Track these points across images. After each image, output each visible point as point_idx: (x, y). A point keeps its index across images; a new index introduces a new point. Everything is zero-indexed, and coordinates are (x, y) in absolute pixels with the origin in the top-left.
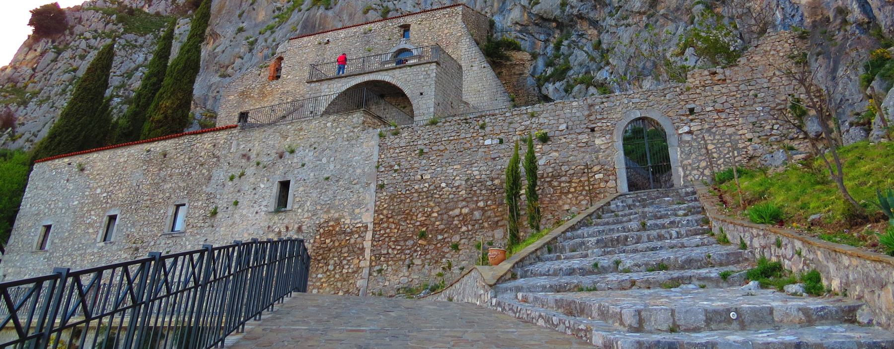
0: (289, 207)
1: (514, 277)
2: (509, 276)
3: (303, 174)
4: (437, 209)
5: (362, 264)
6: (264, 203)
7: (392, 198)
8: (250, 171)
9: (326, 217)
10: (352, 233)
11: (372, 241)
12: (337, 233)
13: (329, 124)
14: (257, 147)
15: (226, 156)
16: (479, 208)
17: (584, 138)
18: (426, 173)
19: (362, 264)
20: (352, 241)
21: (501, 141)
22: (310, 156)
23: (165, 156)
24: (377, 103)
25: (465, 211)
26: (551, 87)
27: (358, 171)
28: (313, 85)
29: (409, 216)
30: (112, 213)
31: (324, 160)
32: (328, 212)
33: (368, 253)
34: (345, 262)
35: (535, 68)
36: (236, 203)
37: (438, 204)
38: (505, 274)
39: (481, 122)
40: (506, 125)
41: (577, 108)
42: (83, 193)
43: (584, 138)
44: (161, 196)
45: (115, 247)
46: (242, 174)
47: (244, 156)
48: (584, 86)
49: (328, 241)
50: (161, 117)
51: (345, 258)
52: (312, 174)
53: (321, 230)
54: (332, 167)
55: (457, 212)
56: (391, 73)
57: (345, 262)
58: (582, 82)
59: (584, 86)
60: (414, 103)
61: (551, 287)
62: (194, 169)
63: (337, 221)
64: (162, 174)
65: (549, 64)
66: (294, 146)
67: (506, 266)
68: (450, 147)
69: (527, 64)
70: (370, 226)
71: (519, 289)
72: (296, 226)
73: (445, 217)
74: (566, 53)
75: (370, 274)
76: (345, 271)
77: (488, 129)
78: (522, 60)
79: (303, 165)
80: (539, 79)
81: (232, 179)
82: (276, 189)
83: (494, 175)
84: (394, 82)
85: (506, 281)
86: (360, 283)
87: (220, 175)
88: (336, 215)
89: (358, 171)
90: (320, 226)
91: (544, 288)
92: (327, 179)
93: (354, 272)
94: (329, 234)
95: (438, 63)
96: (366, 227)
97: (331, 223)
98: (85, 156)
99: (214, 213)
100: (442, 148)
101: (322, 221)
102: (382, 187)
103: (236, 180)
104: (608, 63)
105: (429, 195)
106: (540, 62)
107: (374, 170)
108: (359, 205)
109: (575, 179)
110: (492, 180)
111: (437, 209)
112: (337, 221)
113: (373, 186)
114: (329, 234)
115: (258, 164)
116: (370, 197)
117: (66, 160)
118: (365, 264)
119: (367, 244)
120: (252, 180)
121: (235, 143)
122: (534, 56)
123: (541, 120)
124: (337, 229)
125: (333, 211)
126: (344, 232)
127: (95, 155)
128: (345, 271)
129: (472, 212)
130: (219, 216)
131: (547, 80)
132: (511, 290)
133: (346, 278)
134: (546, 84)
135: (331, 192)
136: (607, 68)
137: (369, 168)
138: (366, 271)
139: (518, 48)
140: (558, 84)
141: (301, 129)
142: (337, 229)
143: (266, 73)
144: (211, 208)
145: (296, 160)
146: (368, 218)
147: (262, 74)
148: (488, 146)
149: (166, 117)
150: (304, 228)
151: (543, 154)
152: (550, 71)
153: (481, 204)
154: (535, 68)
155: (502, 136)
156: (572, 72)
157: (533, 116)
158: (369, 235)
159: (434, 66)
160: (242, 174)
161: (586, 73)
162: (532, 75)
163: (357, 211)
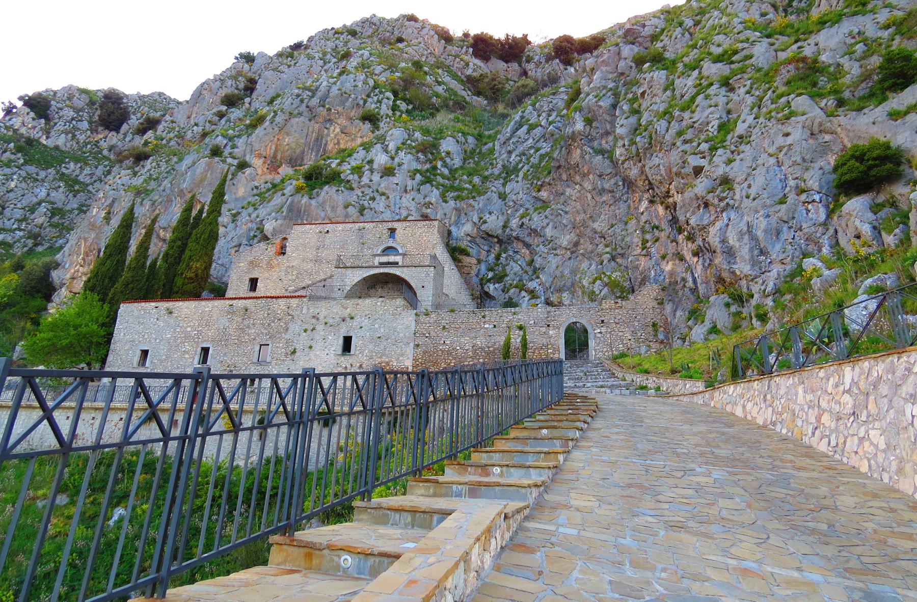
0: (352, 352)
3: (361, 333)
7: (425, 352)
8: (320, 327)
9: (379, 360)
14: (323, 313)
15: (298, 316)
18: (448, 340)
21: (495, 326)
27: (401, 335)
31: (377, 326)
32: (381, 357)
36: (311, 347)
46: (313, 329)
47: (314, 317)
54: (382, 330)
62: (273, 322)
66: (353, 315)
68: (463, 326)
77: (487, 319)
81: (305, 331)
87: (295, 327)
89: (401, 335)
99: (294, 352)
102: (418, 345)
103: (309, 332)
105: (449, 353)
108: (402, 355)
113: (412, 345)
116: (410, 351)
120: (322, 333)
121: (305, 308)
130: (298, 354)
137: (409, 333)
144: (291, 349)
150: (364, 366)
160: (313, 329)
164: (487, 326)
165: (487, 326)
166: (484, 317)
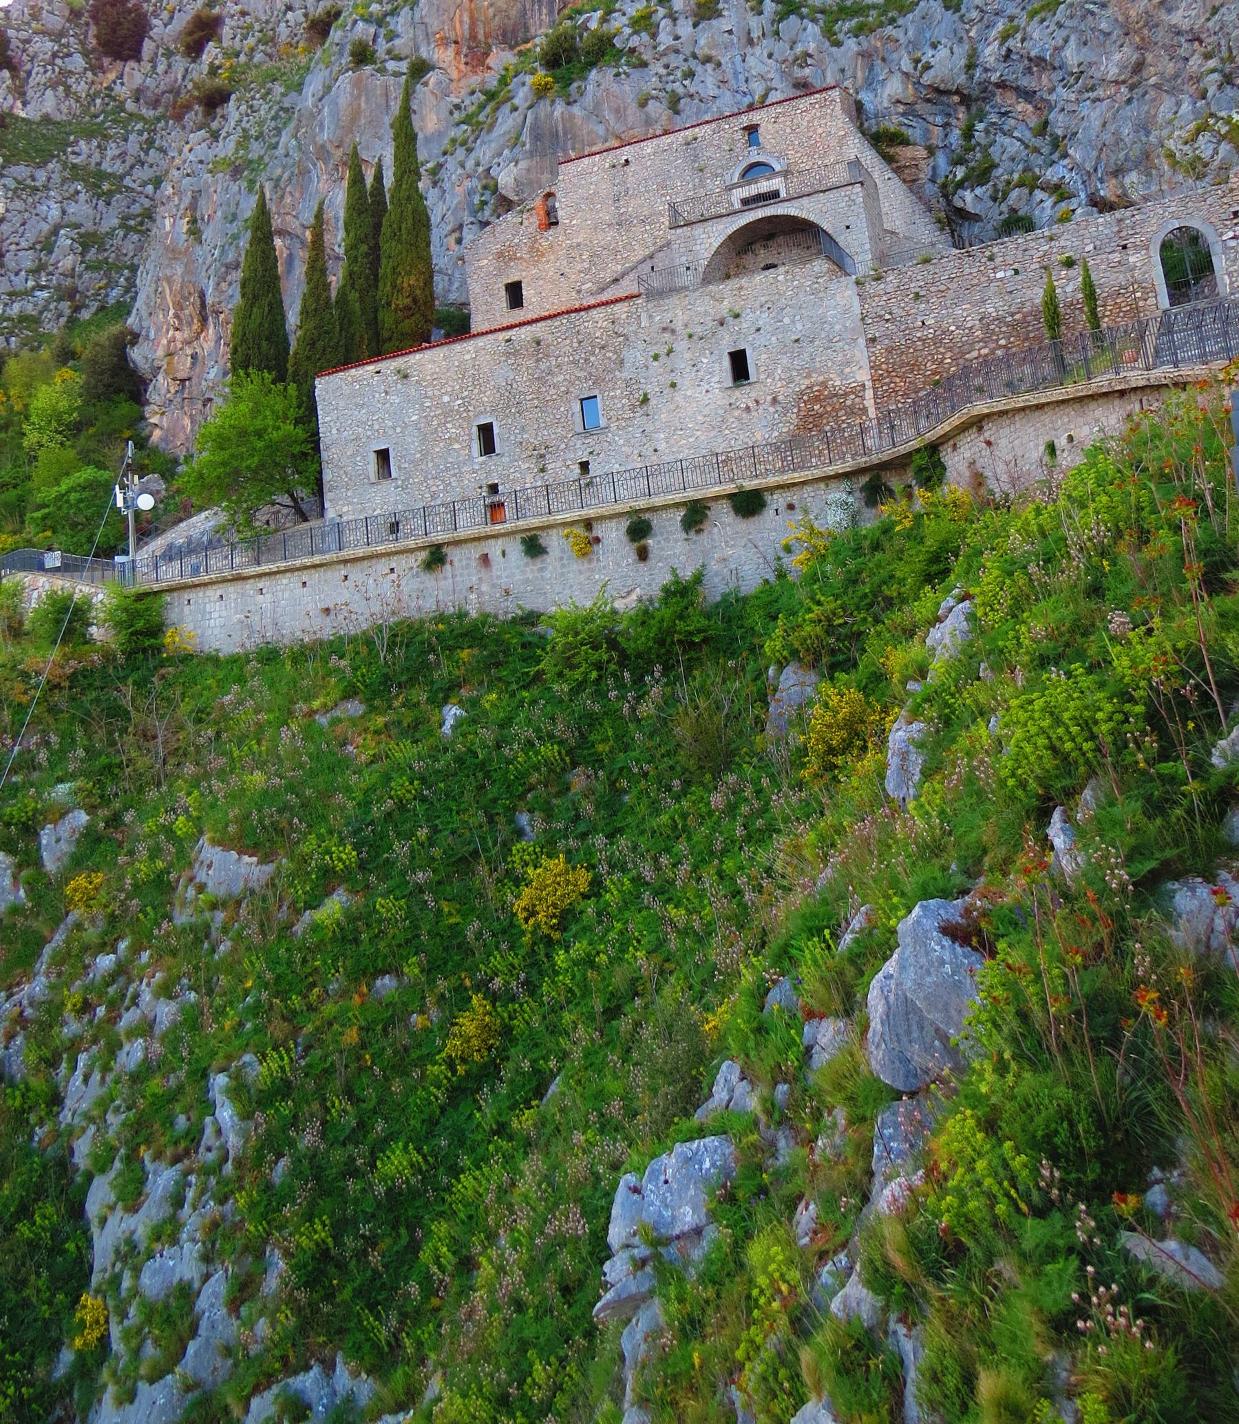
0: (752, 378)
3: (761, 340)
4: (949, 355)
6: (716, 379)
7: (889, 350)
8: (681, 345)
9: (807, 382)
10: (846, 394)
11: (875, 396)
12: (826, 397)
13: (781, 278)
14: (680, 319)
15: (636, 333)
16: (1001, 347)
17: (1116, 257)
18: (931, 317)
20: (849, 403)
21: (1017, 272)
22: (764, 319)
23: (538, 343)
24: (765, 247)
25: (985, 351)
26: (968, 195)
27: (838, 327)
28: (679, 231)
29: (915, 366)
31: (786, 320)
32: (808, 376)
33: (872, 413)
35: (934, 169)
36: (673, 385)
37: (950, 349)
39: (988, 253)
40: (1020, 253)
41: (1106, 224)
43: (1116, 257)
44: (552, 391)
45: (505, 459)
46: (670, 351)
47: (665, 329)
48: (1026, 191)
50: (408, 301)
54: (799, 327)
55: (975, 354)
56: (796, 203)
58: (1020, 185)
59: (1026, 191)
60: (841, 240)
62: (593, 354)
63: (824, 384)
64: (543, 366)
65: (960, 161)
66: (737, 310)
68: (953, 286)
69: (922, 164)
70: (869, 384)
72: (769, 398)
73: (961, 361)
74: (983, 142)
77: (998, 260)
78: (913, 159)
80: (944, 186)
81: (656, 358)
82: (726, 363)
83: (1013, 309)
84: (804, 215)
87: (635, 356)
88: (821, 379)
89: (838, 327)
90: (802, 393)
92: (797, 341)
94: (817, 399)
95: (862, 183)
96: (863, 385)
98: (406, 359)
99: (645, 400)
100: (943, 288)
102: (873, 340)
103: (663, 359)
104: (1065, 156)
105: (937, 341)
106: (941, 160)
107: (859, 323)
108: (848, 363)
109: (1110, 302)
110: (1012, 315)
111: (949, 355)
113: (862, 341)
114: (817, 399)
115: (690, 336)
116: (860, 353)
117: (371, 368)
119: (869, 403)
120: (687, 355)
121: (644, 317)
122: (931, 151)
123: (1063, 243)
126: (836, 395)
127: (418, 356)
129: (992, 352)
130: (653, 402)
131: (960, 185)
134: (960, 192)
136: (1066, 162)
137: (852, 321)
139: (905, 142)
140: (978, 191)
141: (741, 288)
143: (533, 221)
144: (639, 395)
145: (745, 324)
146: (864, 376)
147: (526, 223)
148: (1001, 280)
149: (415, 301)
150: (781, 398)
151: (1070, 280)
152: (960, 172)
153: (1003, 342)
154: (934, 169)
155: (1016, 266)
156: (1000, 171)
157: (1052, 239)
158: (869, 394)
159: (858, 188)
160: (670, 351)
161: (1024, 171)
162: (933, 181)
163: (847, 370)
164: (1000, 275)
165: (1000, 275)
166: (991, 259)
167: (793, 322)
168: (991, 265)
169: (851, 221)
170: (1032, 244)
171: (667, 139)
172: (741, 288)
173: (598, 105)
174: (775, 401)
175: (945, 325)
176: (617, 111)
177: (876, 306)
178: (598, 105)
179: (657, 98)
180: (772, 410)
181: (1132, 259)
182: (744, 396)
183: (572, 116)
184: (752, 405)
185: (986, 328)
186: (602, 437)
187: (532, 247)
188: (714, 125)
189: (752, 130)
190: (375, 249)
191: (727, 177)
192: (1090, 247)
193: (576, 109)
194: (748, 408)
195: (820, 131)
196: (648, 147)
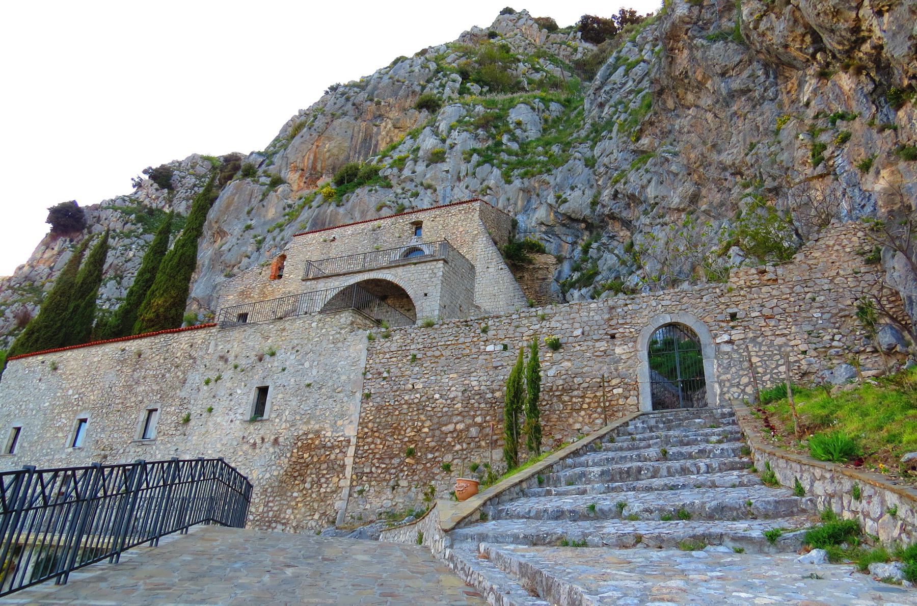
0: (265, 417)
1: (484, 518)
2: (477, 516)
3: (282, 379)
4: (428, 423)
5: (342, 483)
6: (240, 411)
7: (379, 409)
8: (227, 374)
9: (305, 428)
10: (332, 448)
11: (355, 457)
13: (314, 325)
14: (236, 348)
16: (476, 424)
17: (602, 346)
19: (342, 483)
20: (333, 457)
21: (505, 348)
23: (140, 356)
25: (460, 426)
27: (344, 378)
28: (309, 283)
29: (396, 430)
30: (83, 417)
31: (307, 365)
33: (349, 471)
34: (323, 480)
35: (560, 272)
36: (210, 410)
37: (430, 418)
38: (471, 514)
39: (483, 325)
40: (511, 328)
41: (596, 311)
42: (55, 394)
44: (133, 399)
45: (83, 454)
46: (219, 378)
47: (221, 357)
49: (306, 456)
51: (323, 475)
52: (292, 380)
53: (300, 444)
54: (314, 372)
55: (451, 427)
56: (393, 271)
57: (323, 480)
58: (610, 289)
60: (417, 304)
61: (525, 537)
63: (317, 433)
64: (136, 375)
65: (575, 269)
67: (475, 503)
68: (447, 353)
69: (552, 268)
70: (354, 441)
71: (483, 538)
72: (273, 437)
73: (437, 433)
74: (595, 256)
75: (350, 495)
76: (323, 490)
77: (491, 333)
79: (284, 370)
80: (563, 285)
81: (207, 383)
82: (253, 395)
83: (495, 386)
84: (396, 281)
85: (471, 523)
86: (339, 504)
87: (195, 378)
88: (317, 427)
89: (344, 378)
90: (298, 438)
91: (516, 539)
92: (309, 385)
93: (333, 492)
94: (308, 447)
95: (445, 261)
96: (349, 441)
97: (310, 436)
98: (59, 354)
99: (187, 420)
100: (437, 353)
101: (301, 432)
102: (368, 396)
103: (212, 384)
106: (566, 267)
107: (361, 377)
108: (342, 416)
109: (589, 394)
110: (493, 392)
111: (428, 423)
112: (317, 433)
113: (359, 395)
114: (308, 447)
115: (236, 367)
116: (354, 407)
118: (345, 483)
119: (349, 461)
121: (213, 343)
122: (560, 260)
123: (553, 324)
124: (317, 442)
125: (313, 422)
127: (69, 353)
128: (323, 490)
129: (467, 428)
130: (192, 423)
131: (572, 285)
132: (472, 538)
133: (323, 499)
134: (572, 290)
135: (312, 400)
138: (346, 492)
139: (541, 251)
140: (584, 291)
141: (284, 330)
142: (317, 442)
143: (268, 272)
144: (184, 415)
145: (276, 363)
146: (351, 431)
148: (490, 353)
149: (158, 316)
150: (281, 440)
151: (553, 364)
152: (576, 276)
153: (479, 420)
154: (560, 272)
155: (506, 341)
156: (600, 277)
157: (543, 319)
158: (351, 451)
159: (440, 264)
160: (219, 378)
161: (616, 278)
162: (557, 280)
163: (340, 423)
164: (490, 348)
165: (490, 348)
166: (485, 331)
167: (311, 366)
168: (484, 337)
169: (429, 290)
170: (525, 322)
171: (361, 226)
172: (284, 330)
173: (353, 207)
174: (276, 441)
175: (431, 392)
176: (363, 212)
177: (377, 363)
178: (353, 207)
179: (390, 207)
180: (271, 450)
181: (618, 350)
182: (255, 432)
183: (337, 214)
184: (259, 441)
185: (466, 401)
186: (148, 448)
187: (262, 291)
188: (393, 219)
189: (418, 225)
190: (153, 277)
191: (392, 256)
192: (578, 332)
193: (341, 210)
194: (255, 444)
195: (461, 229)
196: (349, 230)
